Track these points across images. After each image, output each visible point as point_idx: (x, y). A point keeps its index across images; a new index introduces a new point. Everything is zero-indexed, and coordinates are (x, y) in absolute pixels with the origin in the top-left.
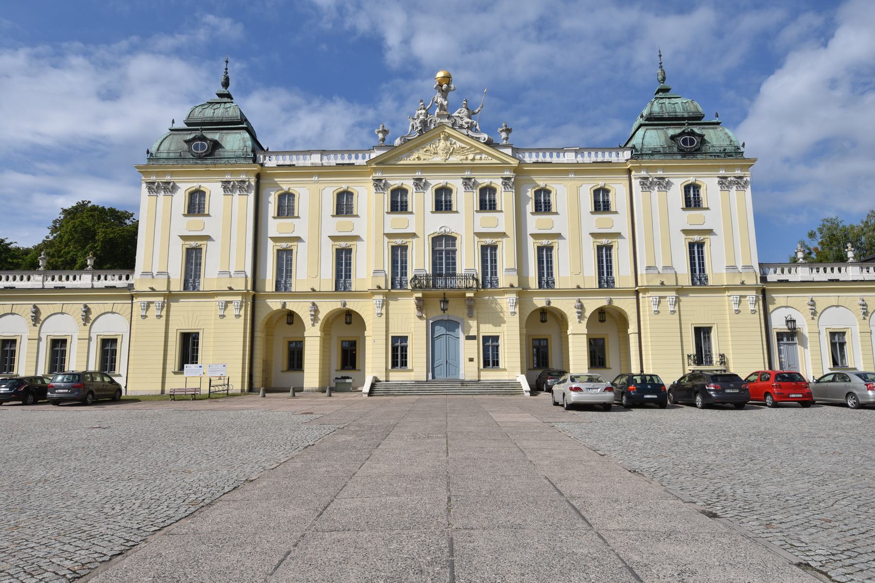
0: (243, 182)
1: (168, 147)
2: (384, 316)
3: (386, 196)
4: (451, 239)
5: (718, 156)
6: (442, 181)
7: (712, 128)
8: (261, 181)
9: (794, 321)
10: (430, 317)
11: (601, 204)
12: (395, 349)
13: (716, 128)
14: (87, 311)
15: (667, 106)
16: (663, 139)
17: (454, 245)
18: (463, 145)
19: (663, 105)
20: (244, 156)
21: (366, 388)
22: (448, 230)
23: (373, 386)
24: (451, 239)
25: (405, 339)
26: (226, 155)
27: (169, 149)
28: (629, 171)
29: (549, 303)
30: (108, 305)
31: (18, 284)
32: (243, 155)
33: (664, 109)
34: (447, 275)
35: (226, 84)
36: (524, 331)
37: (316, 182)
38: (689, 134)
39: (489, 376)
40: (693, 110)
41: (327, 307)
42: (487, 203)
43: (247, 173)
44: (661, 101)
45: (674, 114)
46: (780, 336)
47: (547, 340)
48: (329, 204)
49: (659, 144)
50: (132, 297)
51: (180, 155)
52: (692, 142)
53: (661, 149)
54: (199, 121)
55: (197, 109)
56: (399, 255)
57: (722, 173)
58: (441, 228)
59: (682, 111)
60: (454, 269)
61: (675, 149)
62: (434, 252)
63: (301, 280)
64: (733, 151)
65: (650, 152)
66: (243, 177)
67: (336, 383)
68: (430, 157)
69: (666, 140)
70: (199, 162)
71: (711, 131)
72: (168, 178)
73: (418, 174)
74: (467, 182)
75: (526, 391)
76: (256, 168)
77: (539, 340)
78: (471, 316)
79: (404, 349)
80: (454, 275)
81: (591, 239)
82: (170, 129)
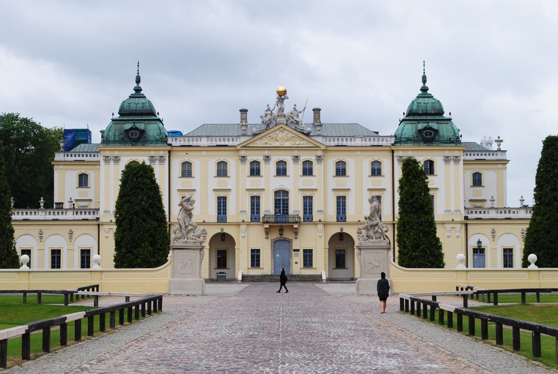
0: (161, 157)
1: (114, 133)
2: (246, 237)
3: (246, 165)
4: (286, 193)
5: (446, 143)
6: (280, 157)
7: (445, 123)
8: (171, 156)
9: (481, 242)
10: (273, 239)
11: (376, 171)
12: (252, 257)
13: (447, 123)
14: (71, 233)
15: (422, 105)
16: (414, 131)
17: (287, 195)
18: (293, 135)
19: (420, 104)
20: (160, 140)
21: (240, 278)
22: (283, 187)
23: (243, 277)
24: (286, 193)
25: (258, 251)
26: (150, 139)
27: (115, 135)
28: (393, 151)
29: (342, 230)
30: (85, 229)
31: (29, 217)
32: (160, 139)
33: (420, 108)
34: (284, 213)
35: (138, 81)
36: (327, 246)
37: (204, 156)
38: (428, 129)
39: (308, 272)
40: (438, 108)
41: (212, 231)
42: (308, 171)
43: (164, 150)
44: (420, 100)
45: (425, 111)
46: (475, 251)
47: (345, 250)
48: (213, 170)
49: (411, 135)
50: (99, 225)
51: (122, 139)
52: (430, 134)
53: (412, 138)
54: (127, 112)
55: (125, 103)
56: (255, 202)
57: (447, 153)
58: (280, 185)
59: (431, 109)
60: (287, 210)
61: (420, 138)
62: (276, 200)
63: (198, 215)
64: (455, 140)
65: (406, 140)
66: (161, 153)
67: (217, 276)
68: (273, 142)
69: (416, 132)
70: (134, 143)
71: (444, 125)
72: (116, 153)
73: (267, 153)
74: (296, 158)
75: (324, 280)
76: (169, 148)
77: (340, 251)
78: (296, 238)
79: (258, 257)
80: (287, 213)
81: (368, 192)
82: (112, 120)
